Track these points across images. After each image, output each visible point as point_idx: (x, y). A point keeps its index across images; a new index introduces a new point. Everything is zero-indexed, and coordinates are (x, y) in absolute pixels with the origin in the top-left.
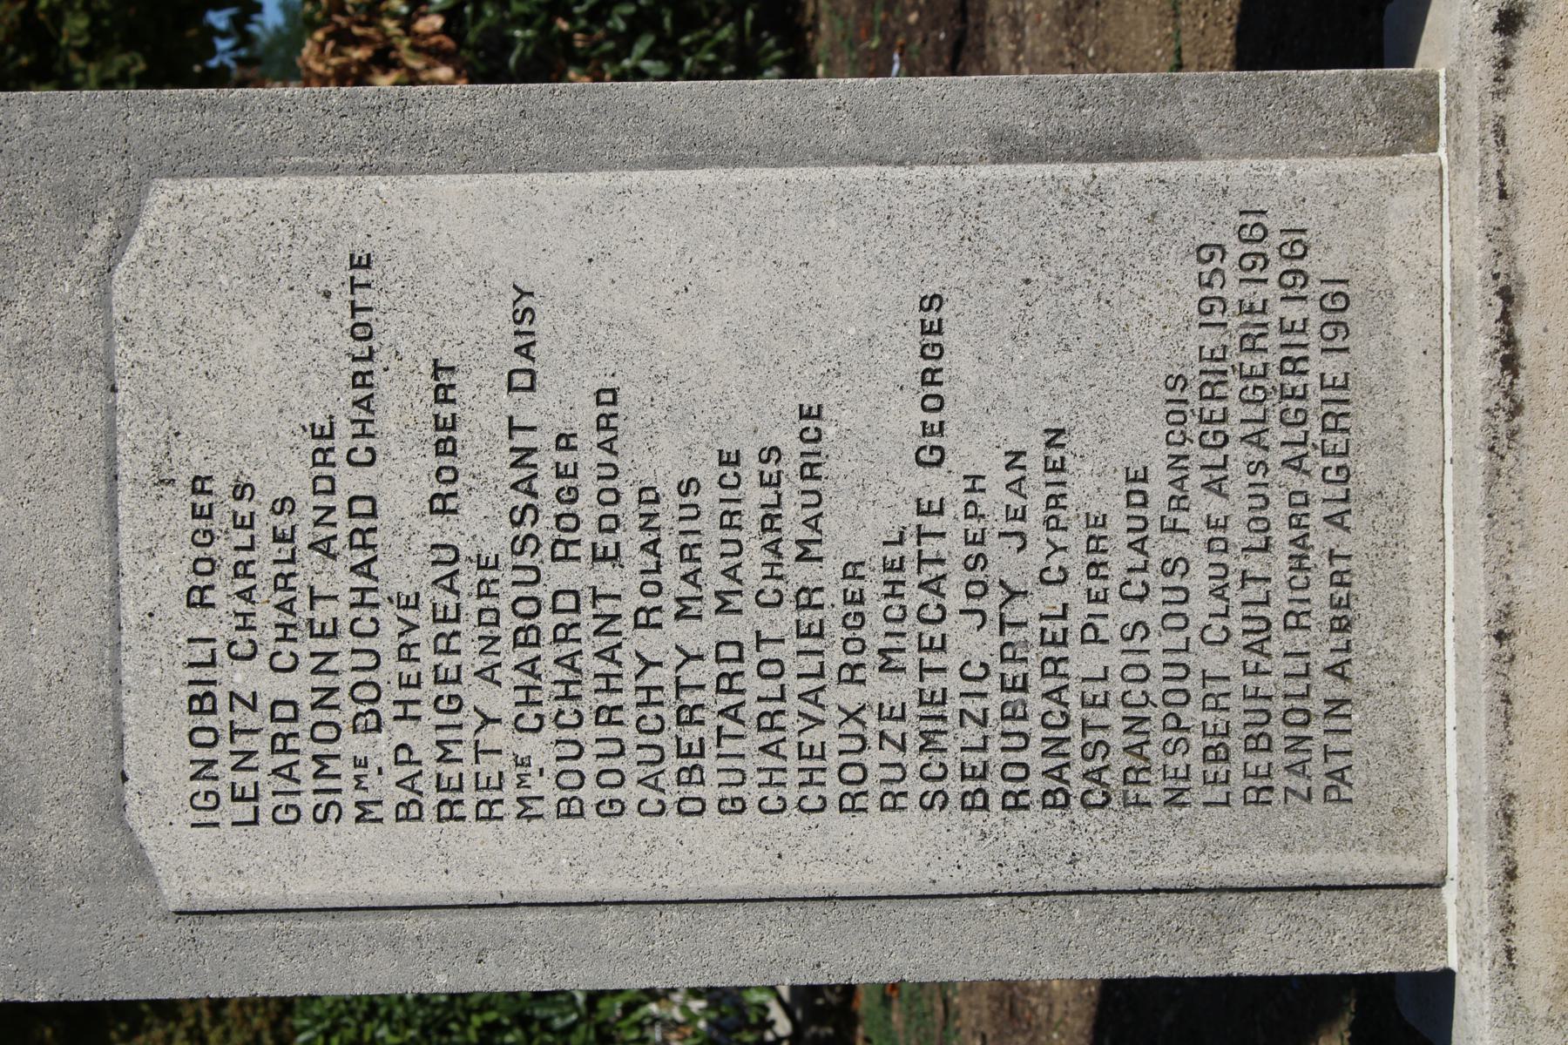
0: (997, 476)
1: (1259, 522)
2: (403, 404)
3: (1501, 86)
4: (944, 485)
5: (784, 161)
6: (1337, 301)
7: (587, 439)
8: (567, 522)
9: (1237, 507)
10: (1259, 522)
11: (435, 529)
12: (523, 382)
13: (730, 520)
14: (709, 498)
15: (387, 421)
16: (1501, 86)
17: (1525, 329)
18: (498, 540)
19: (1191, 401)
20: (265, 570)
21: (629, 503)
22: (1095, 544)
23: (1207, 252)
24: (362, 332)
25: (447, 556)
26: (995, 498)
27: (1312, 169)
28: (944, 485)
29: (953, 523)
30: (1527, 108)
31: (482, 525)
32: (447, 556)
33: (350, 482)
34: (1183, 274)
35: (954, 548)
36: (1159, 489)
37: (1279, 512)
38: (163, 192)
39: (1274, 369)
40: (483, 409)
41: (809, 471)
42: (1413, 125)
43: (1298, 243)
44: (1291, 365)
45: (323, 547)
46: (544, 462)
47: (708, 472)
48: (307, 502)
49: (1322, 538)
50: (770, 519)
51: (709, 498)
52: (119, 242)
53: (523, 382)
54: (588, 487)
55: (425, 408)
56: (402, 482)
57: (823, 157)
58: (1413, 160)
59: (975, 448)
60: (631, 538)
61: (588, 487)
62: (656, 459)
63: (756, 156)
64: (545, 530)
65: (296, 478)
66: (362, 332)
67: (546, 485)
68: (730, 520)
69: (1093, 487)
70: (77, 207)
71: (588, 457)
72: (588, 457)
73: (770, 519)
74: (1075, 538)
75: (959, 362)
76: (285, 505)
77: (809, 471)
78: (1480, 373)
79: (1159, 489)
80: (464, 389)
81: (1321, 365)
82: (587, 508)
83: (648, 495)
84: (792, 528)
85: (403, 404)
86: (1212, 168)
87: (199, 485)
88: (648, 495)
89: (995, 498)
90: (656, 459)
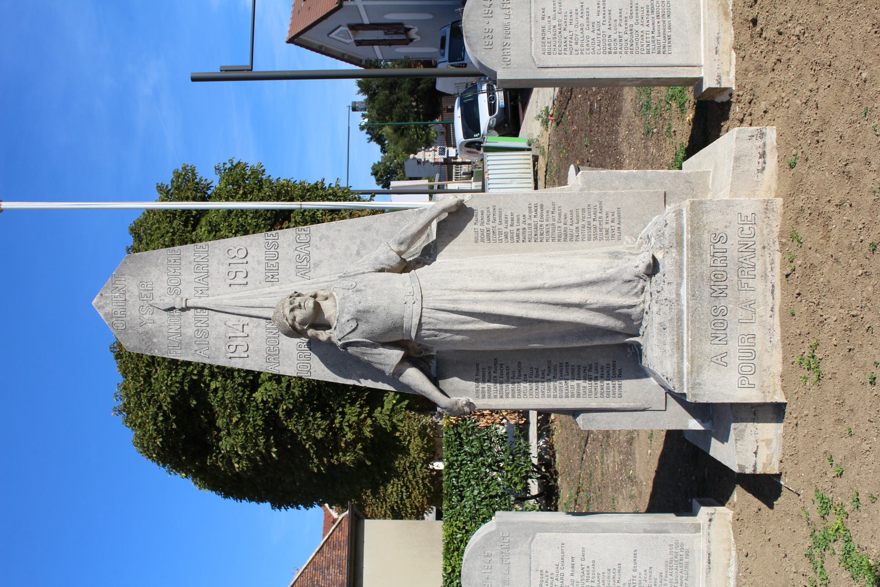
0: (643, 573)
1: (676, 579)
2: (568, 562)
3: (709, 528)
4: (635, 574)
5: (617, 532)
6: (687, 552)
7: (591, 567)
8: (588, 577)
9: (673, 578)
10: (676, 579)
11: (571, 577)
12: (583, 559)
13: (609, 577)
14: (606, 575)
15: (565, 564)
16: (709, 528)
17: (711, 558)
18: (579, 579)
19: (668, 564)
20: (549, 582)
21: (596, 575)
22: (655, 582)
23: (670, 545)
24: (563, 553)
25: (572, 581)
26: (643, 576)
27: (685, 535)
28: (635, 574)
29: (637, 579)
30: (713, 530)
31: (577, 577)
32: (572, 581)
33: (561, 571)
34: (668, 548)
35: (637, 582)
36: (664, 575)
37: (679, 578)
38: (538, 534)
39: (680, 560)
40: (578, 563)
41: (619, 572)
42: (697, 528)
43: (682, 544)
44: (681, 560)
45: (557, 579)
46: (585, 570)
47: (606, 571)
48: (555, 574)
49: (684, 582)
50: (614, 577)
51: (606, 575)
52: (532, 540)
53: (583, 559)
54: (591, 573)
55: (570, 562)
56: (567, 571)
57: (622, 532)
58: (698, 534)
59: (640, 569)
60: (596, 579)
61: (591, 573)
62: (600, 570)
63: (613, 531)
64: (585, 578)
65: (554, 570)
66: (563, 553)
67: (585, 572)
68: (609, 577)
69: (655, 574)
70: (527, 536)
71: (591, 569)
72: (591, 569)
73: (614, 577)
74: (653, 581)
75: (639, 559)
76: (552, 574)
77: (619, 572)
78: (706, 564)
79: (664, 575)
80: (575, 560)
81: (685, 560)
82: (590, 575)
83: (598, 574)
84: (617, 579)
85: (568, 562)
86: (672, 535)
87: (541, 571)
88: (598, 574)
89: (643, 576)
90: (600, 570)
